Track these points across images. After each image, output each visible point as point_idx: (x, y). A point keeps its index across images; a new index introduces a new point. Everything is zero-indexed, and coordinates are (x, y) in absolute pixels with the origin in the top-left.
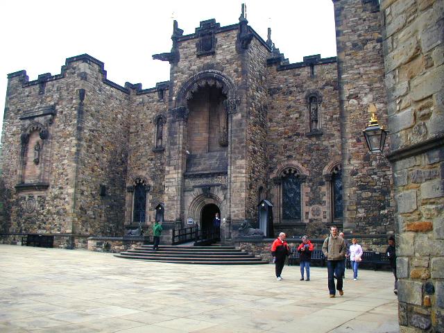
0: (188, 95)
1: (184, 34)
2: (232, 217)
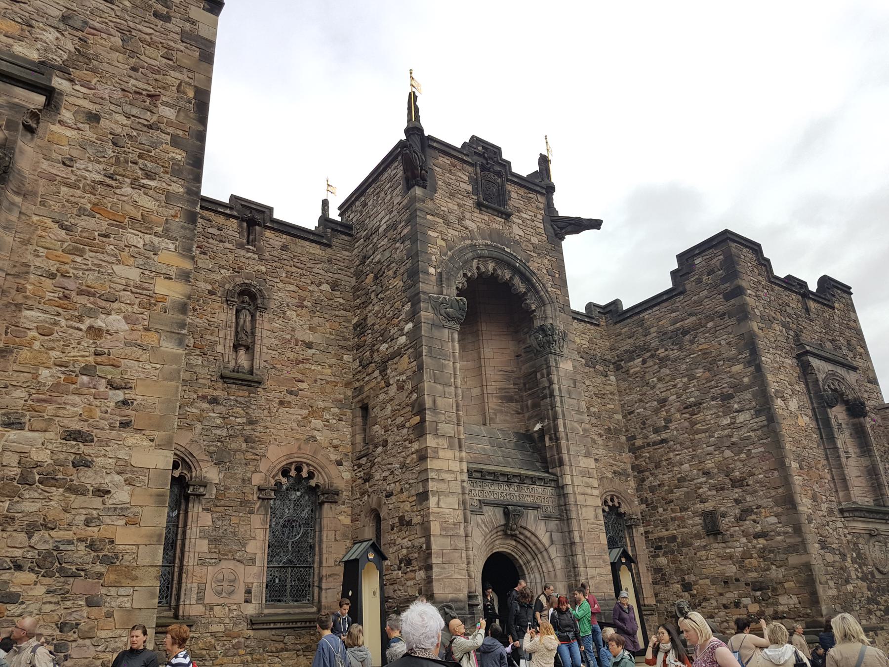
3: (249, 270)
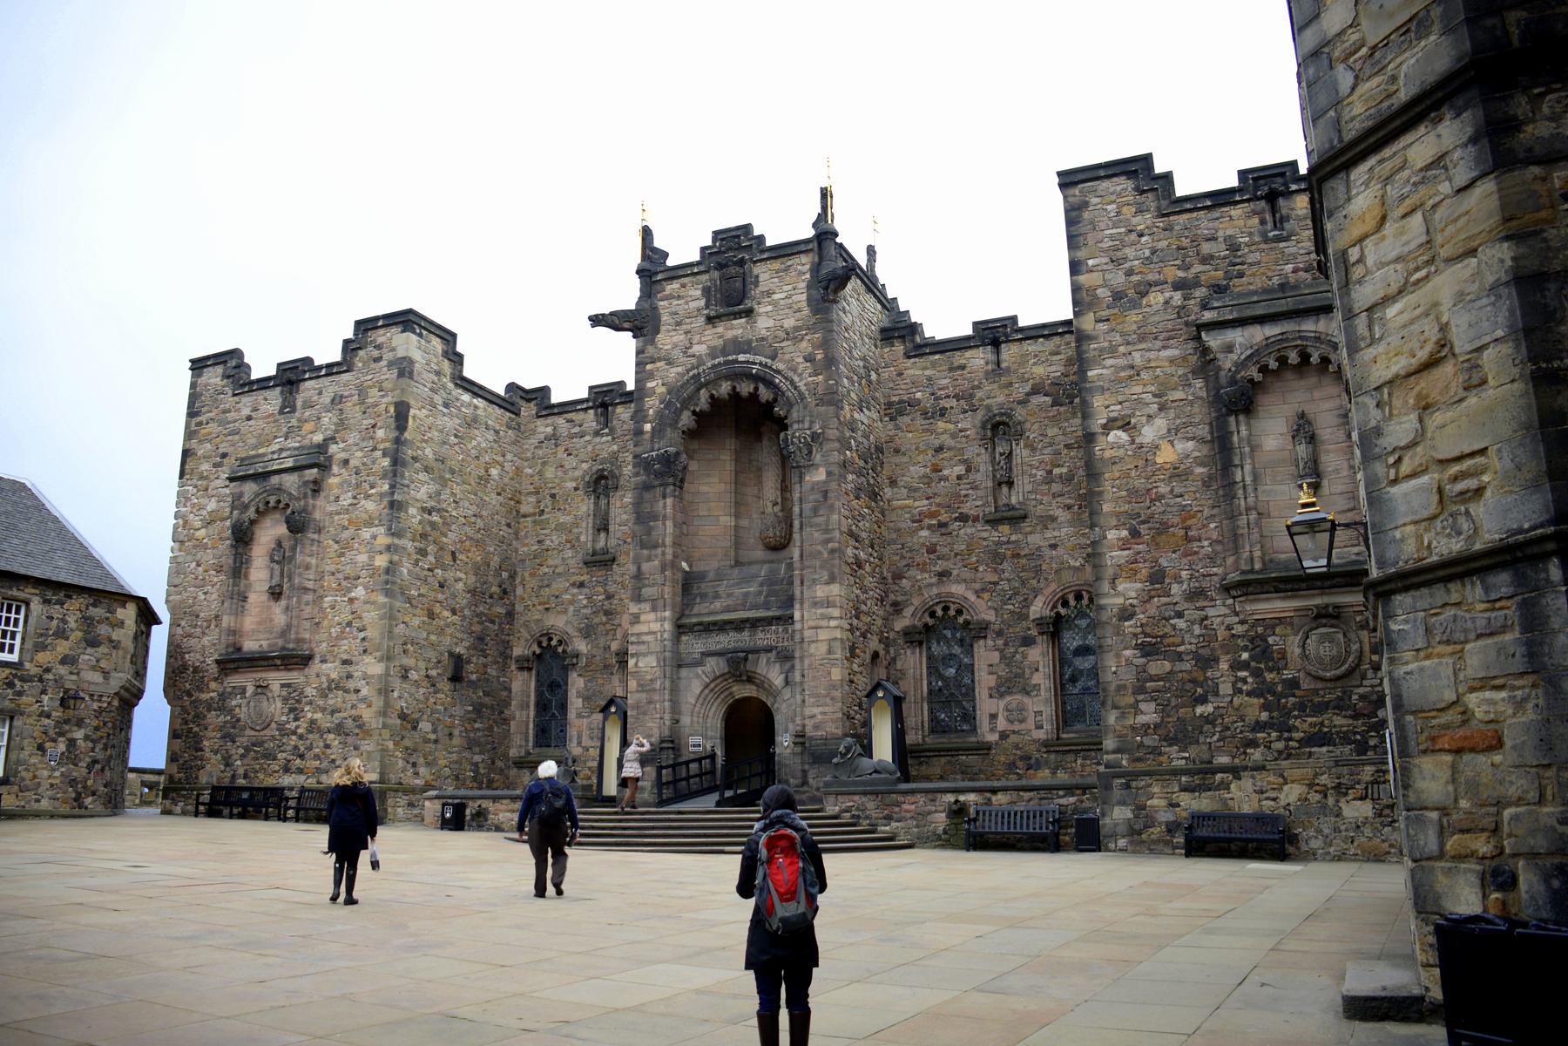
0: (686, 419)
1: (670, 262)
2: (809, 731)
3: (604, 455)
